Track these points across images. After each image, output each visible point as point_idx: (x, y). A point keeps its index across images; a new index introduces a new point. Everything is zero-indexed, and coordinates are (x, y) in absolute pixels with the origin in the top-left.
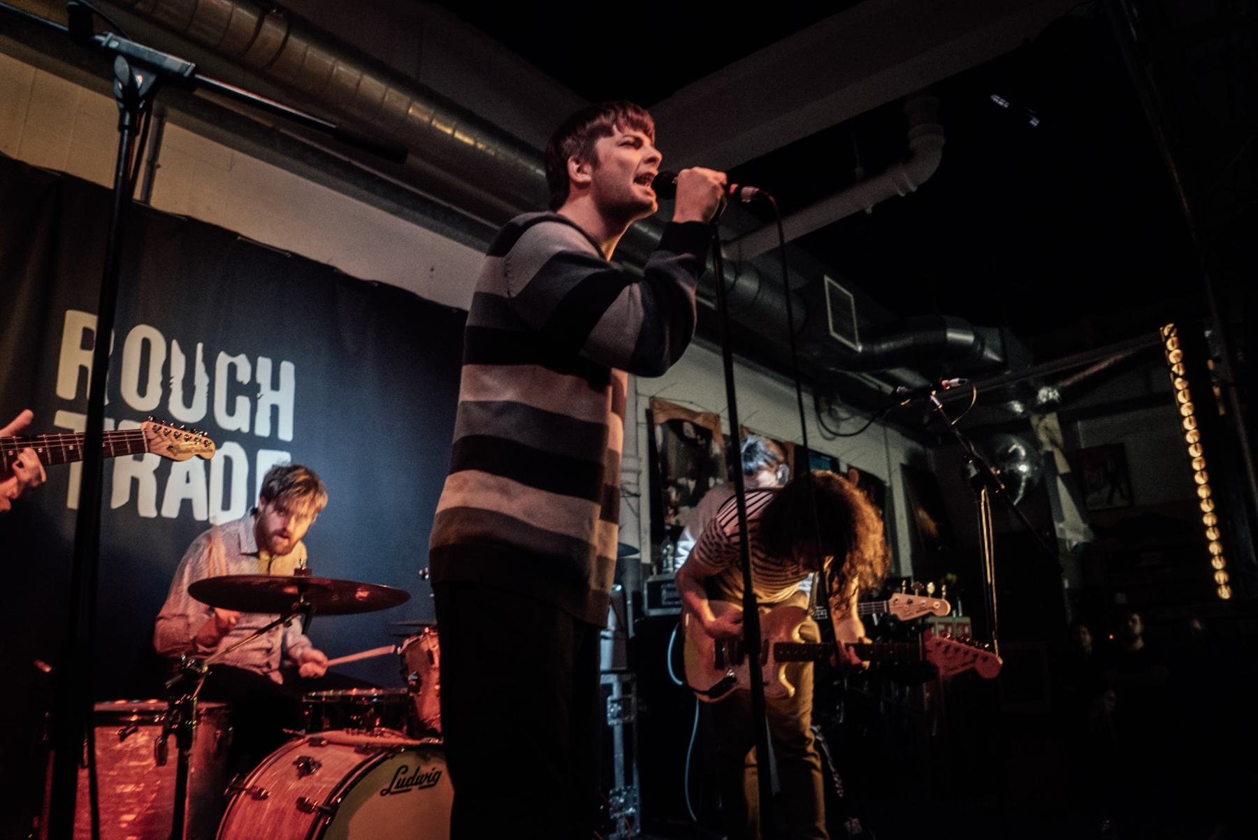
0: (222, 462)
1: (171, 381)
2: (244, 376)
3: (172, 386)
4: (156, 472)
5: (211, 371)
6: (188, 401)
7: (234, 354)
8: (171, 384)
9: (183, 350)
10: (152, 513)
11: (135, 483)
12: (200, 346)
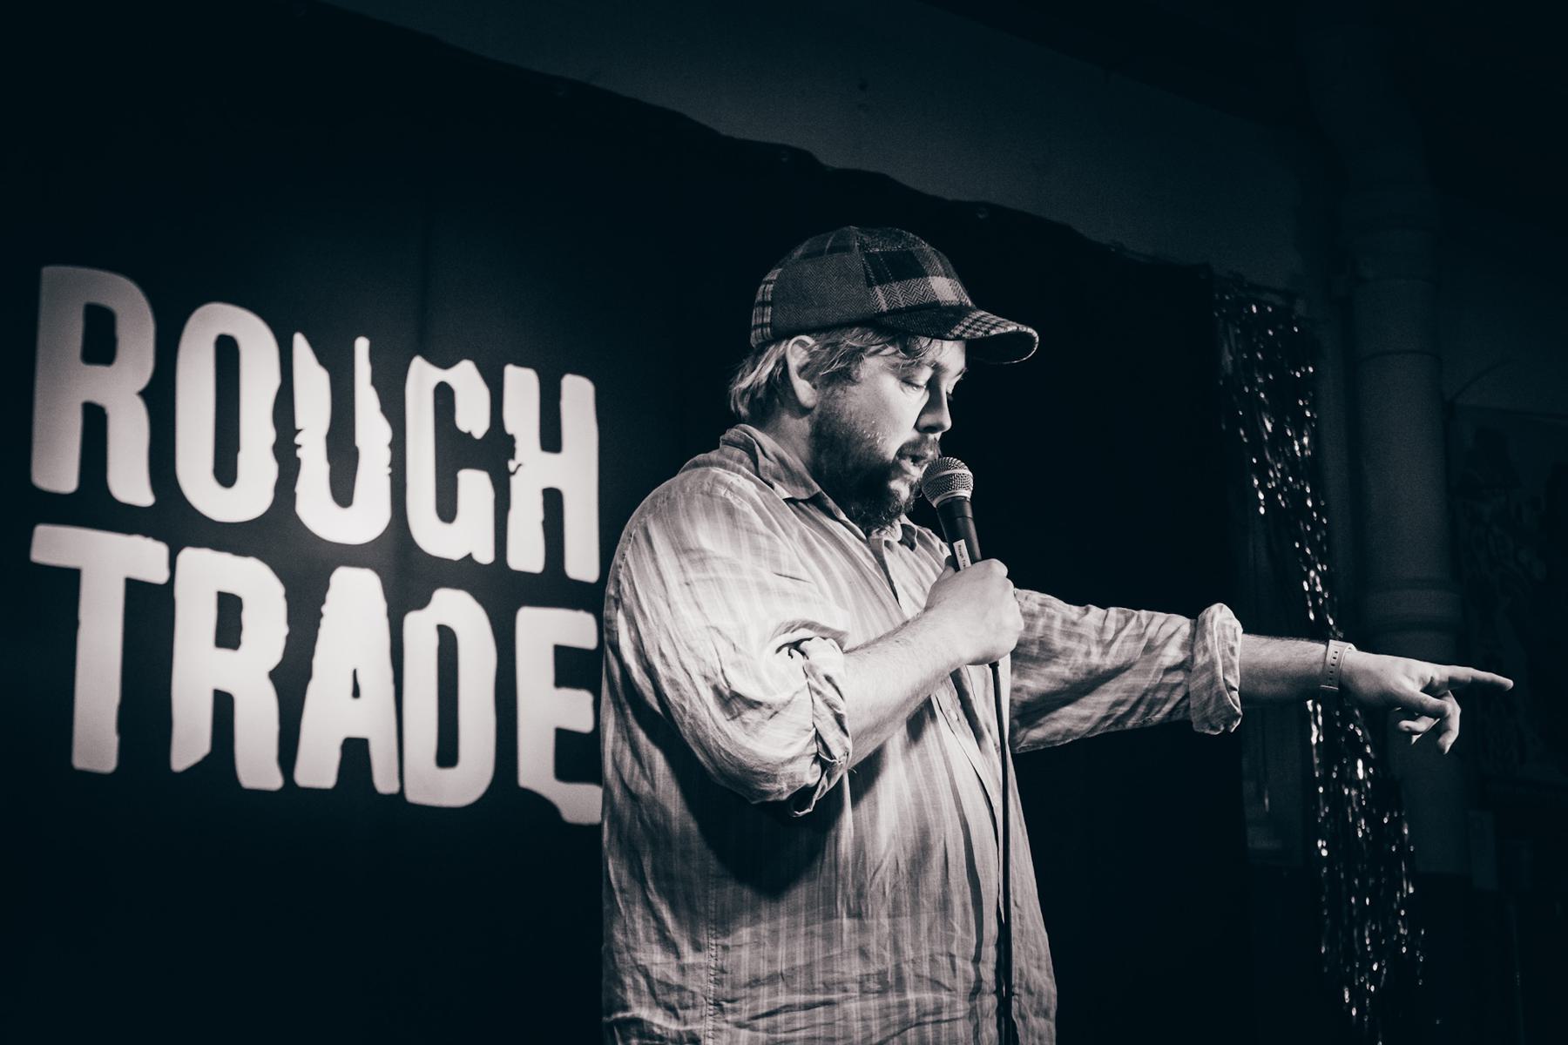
0: (433, 641)
1: (298, 440)
2: (473, 418)
3: (300, 453)
4: (274, 675)
5: (394, 409)
6: (343, 491)
7: (446, 363)
8: (300, 446)
9: (323, 359)
10: (275, 782)
11: (223, 705)
12: (362, 346)
